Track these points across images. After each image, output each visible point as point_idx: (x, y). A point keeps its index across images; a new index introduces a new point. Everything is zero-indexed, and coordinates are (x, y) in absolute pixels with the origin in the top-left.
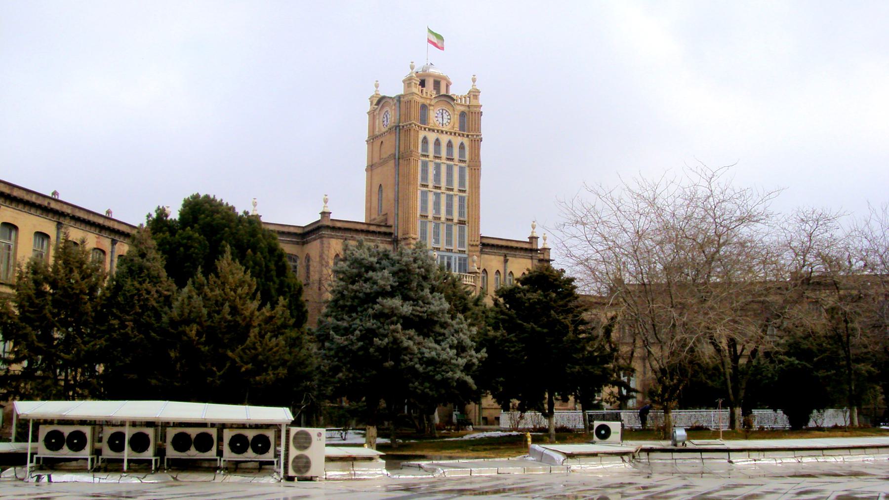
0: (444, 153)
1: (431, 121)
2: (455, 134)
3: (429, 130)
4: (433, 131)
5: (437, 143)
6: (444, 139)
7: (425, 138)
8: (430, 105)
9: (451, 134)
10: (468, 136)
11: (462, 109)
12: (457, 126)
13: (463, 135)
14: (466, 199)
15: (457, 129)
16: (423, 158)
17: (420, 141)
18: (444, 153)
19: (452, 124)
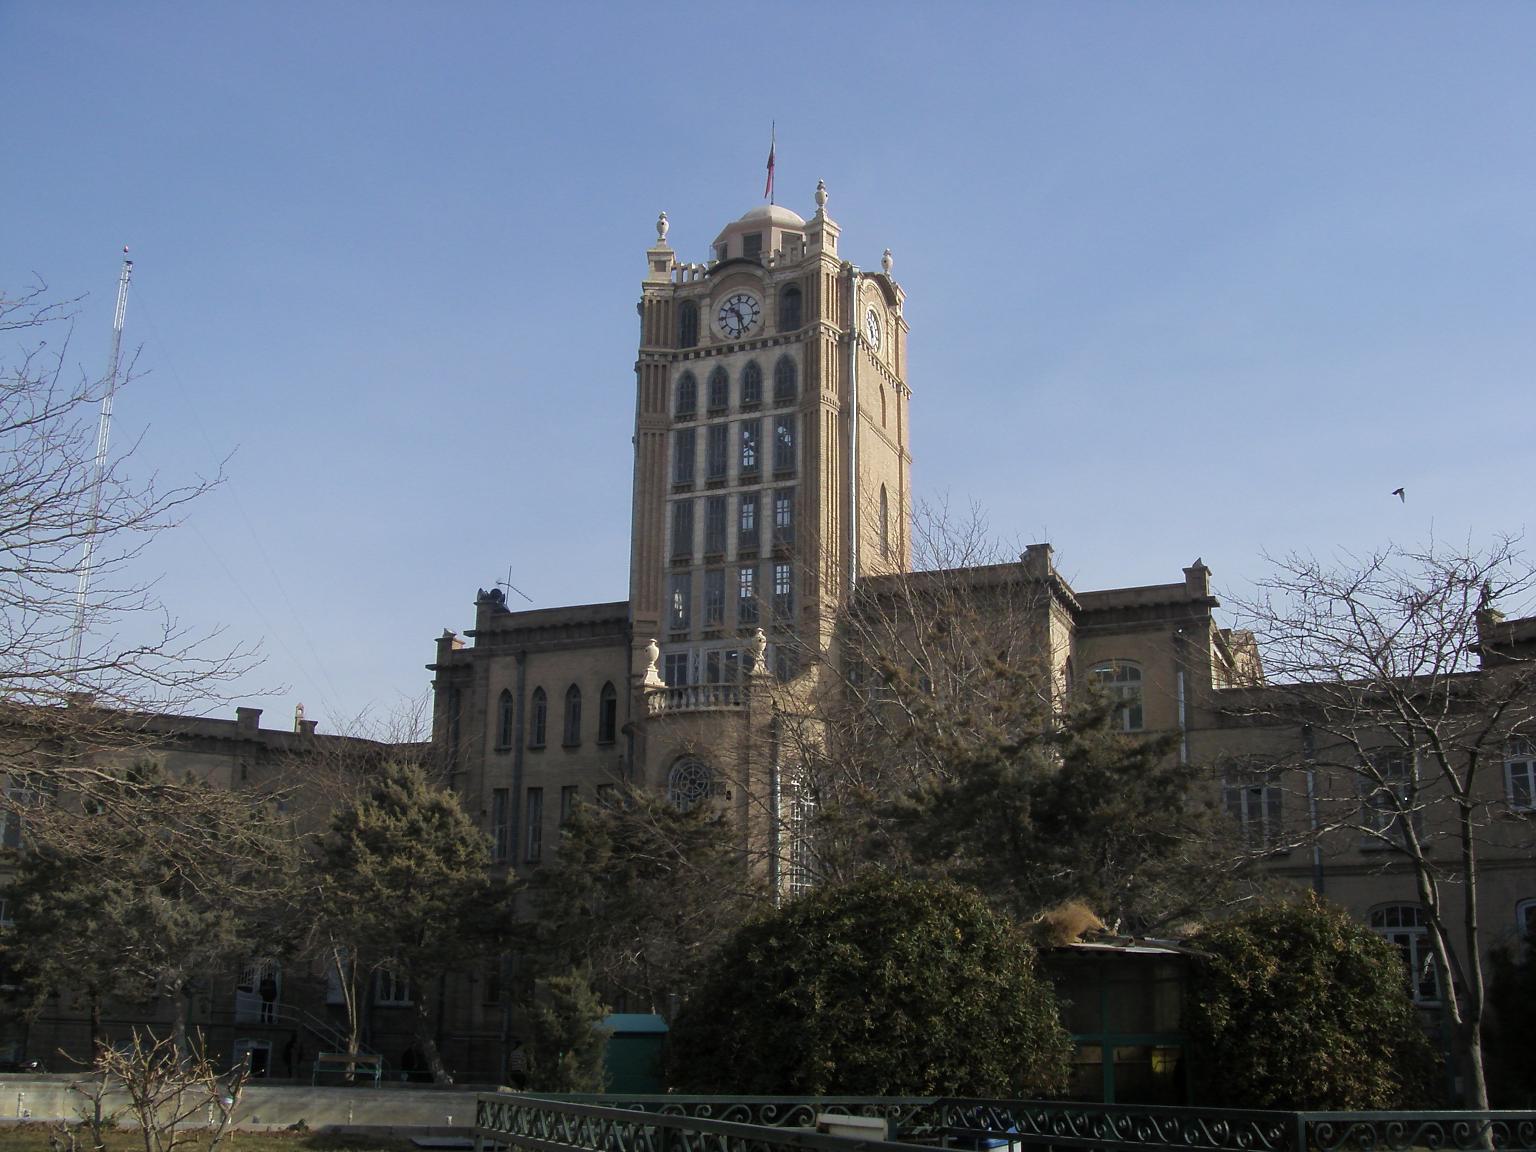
0: (735, 398)
1: (704, 332)
2: (764, 344)
3: (697, 355)
4: (708, 353)
5: (719, 382)
6: (736, 364)
7: (689, 379)
8: (701, 297)
9: (753, 346)
10: (798, 339)
11: (788, 276)
12: (770, 322)
13: (787, 340)
14: (798, 490)
15: (771, 332)
16: (680, 426)
17: (673, 386)
18: (735, 398)
19: (760, 323)
